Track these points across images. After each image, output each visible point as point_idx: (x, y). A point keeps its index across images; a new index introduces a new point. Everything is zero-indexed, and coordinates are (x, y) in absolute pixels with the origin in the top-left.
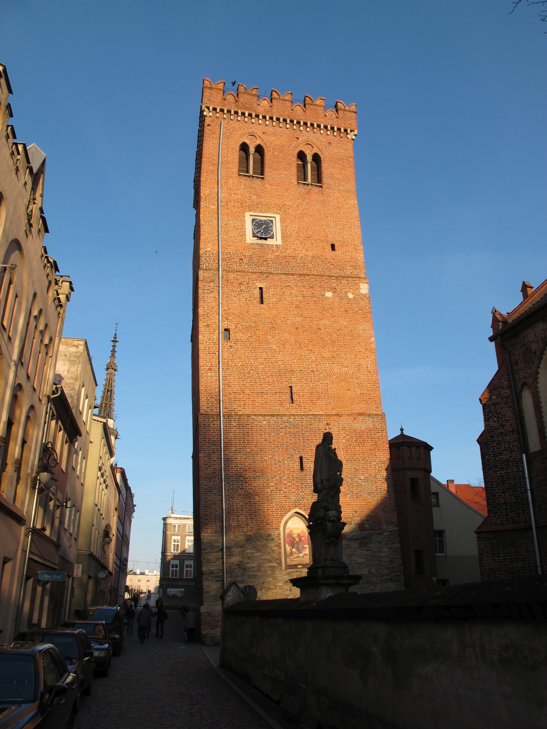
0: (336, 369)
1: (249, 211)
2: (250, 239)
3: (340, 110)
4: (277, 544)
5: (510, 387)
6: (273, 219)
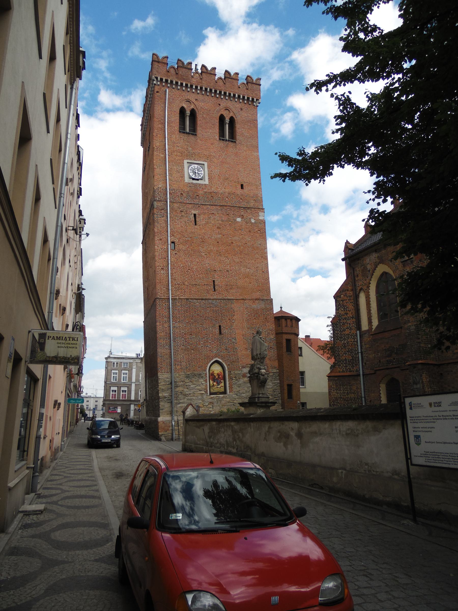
1: (187, 159)
5: (352, 290)
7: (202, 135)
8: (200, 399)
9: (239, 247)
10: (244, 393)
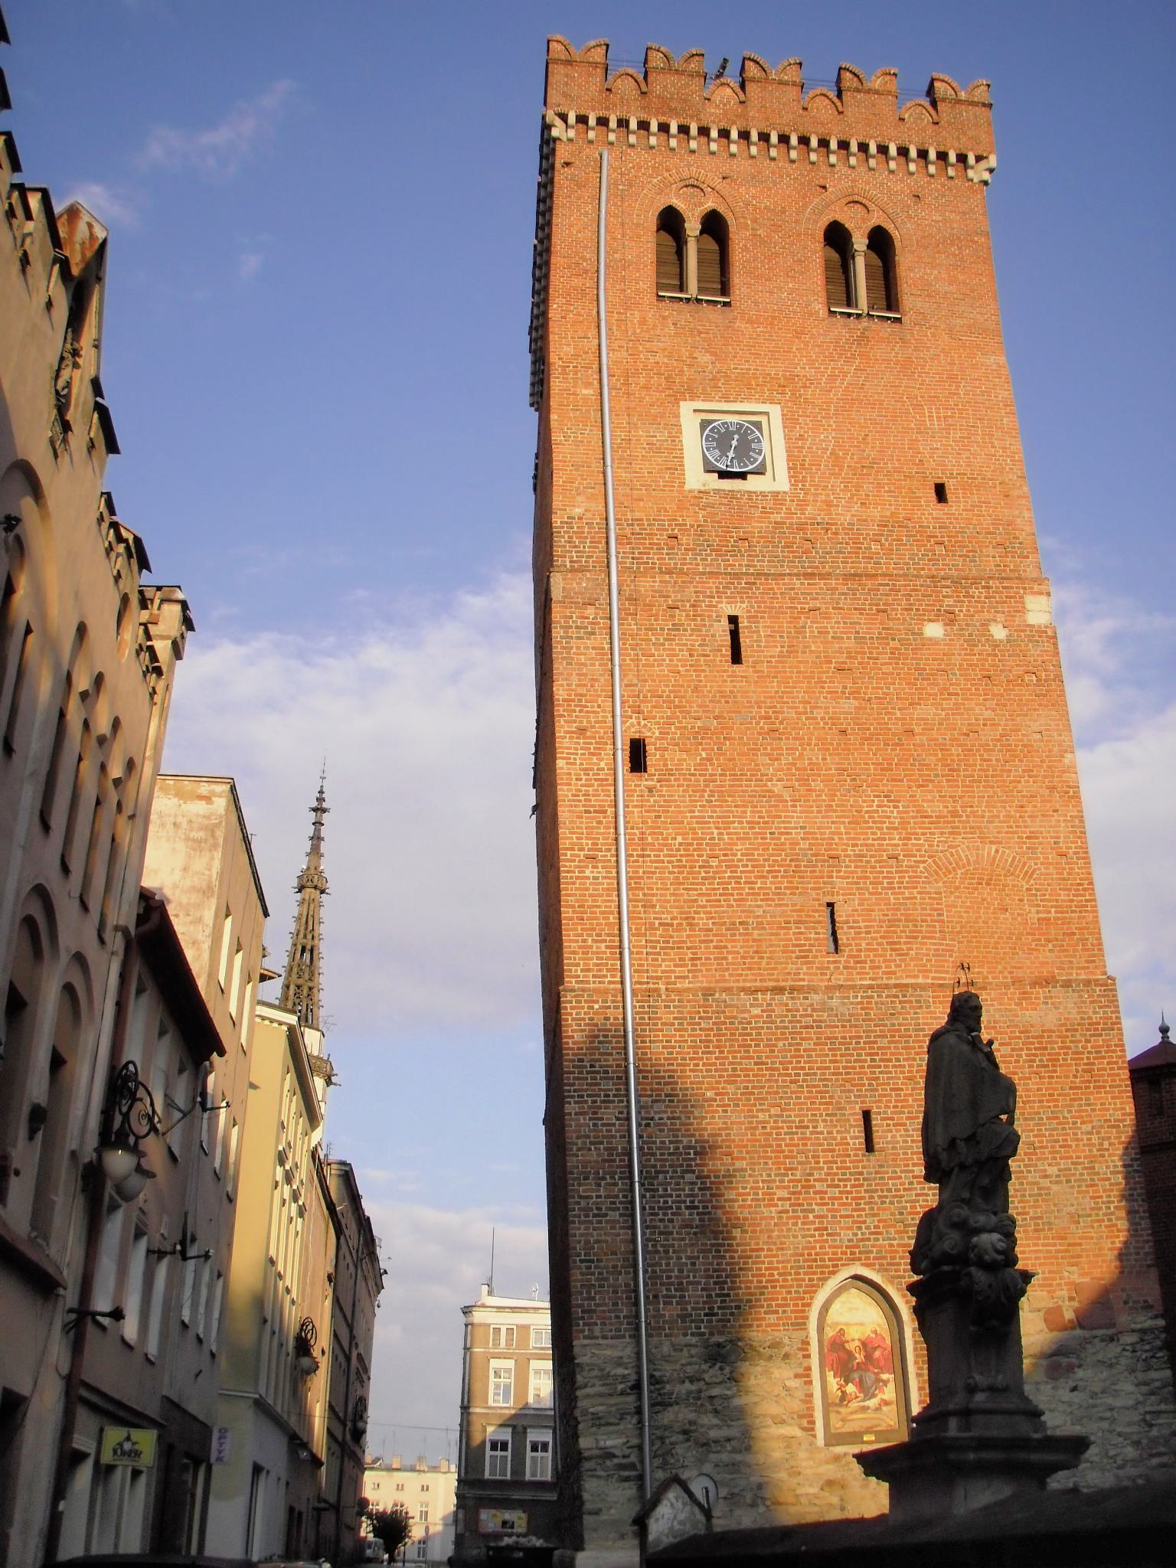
2: (696, 478)
3: (944, 100)
4: (800, 1371)
6: (763, 419)
7: (756, 303)
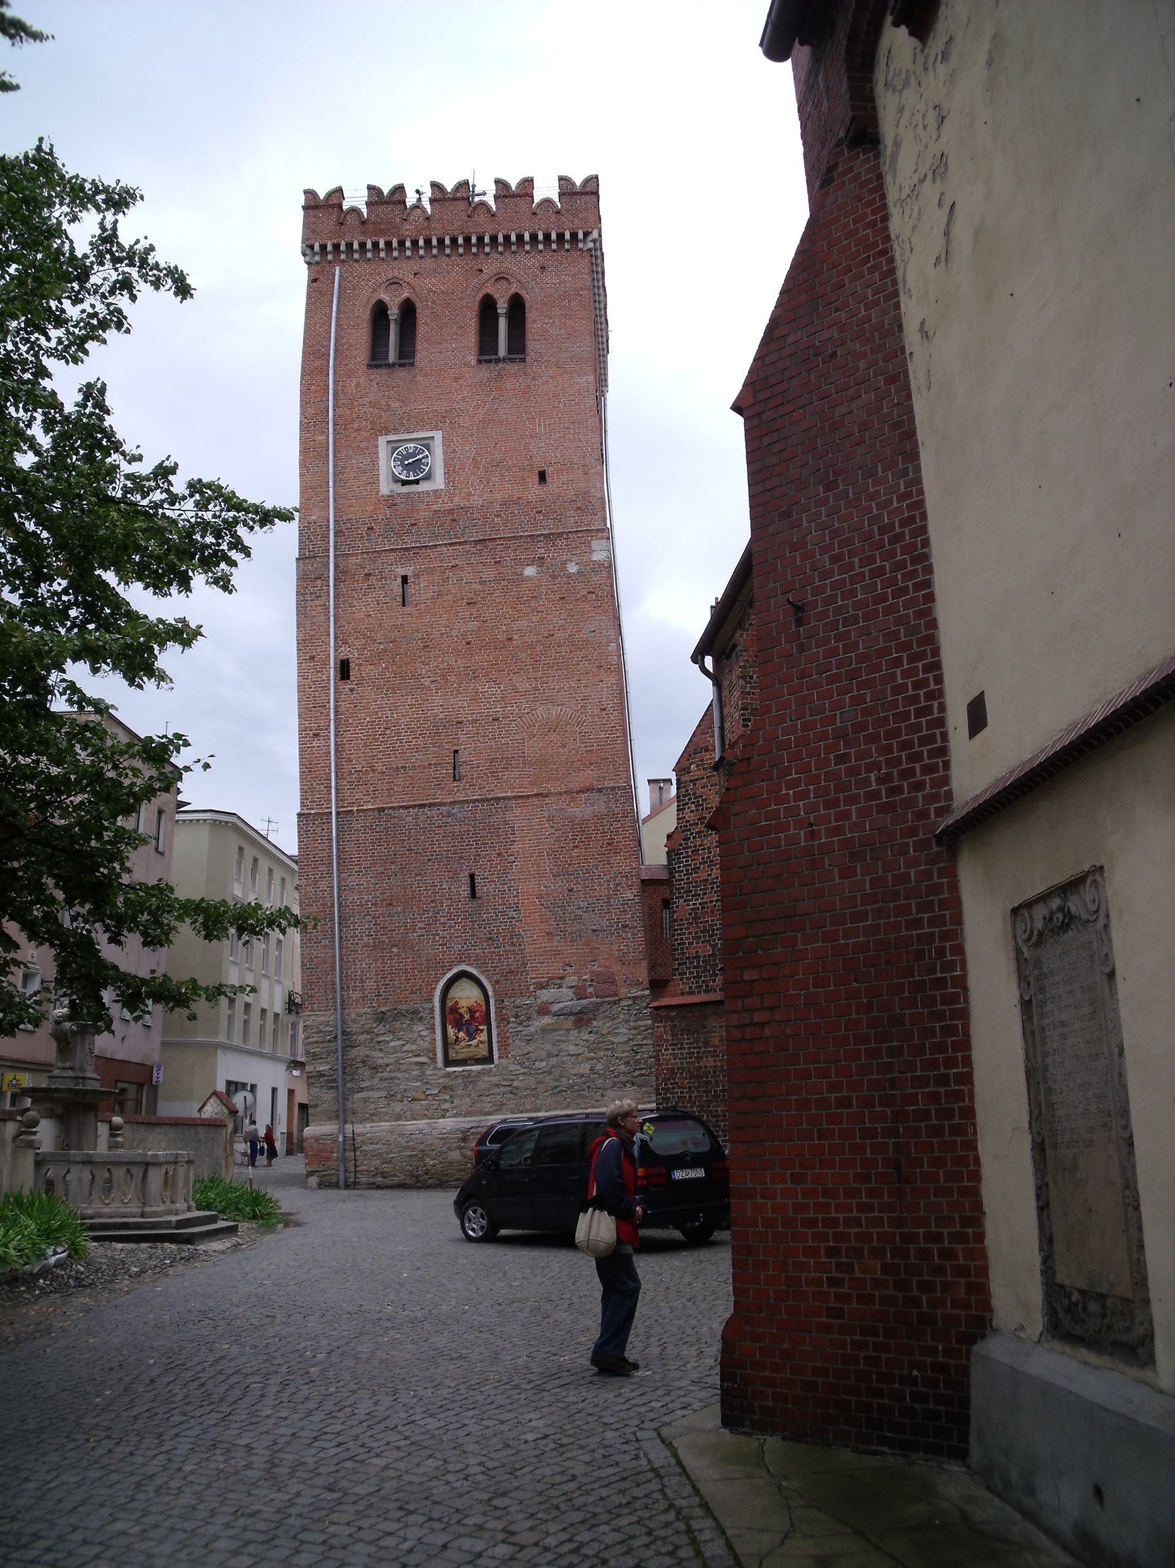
0: (541, 711)
8: (417, 1079)
9: (531, 647)
10: (542, 1060)
